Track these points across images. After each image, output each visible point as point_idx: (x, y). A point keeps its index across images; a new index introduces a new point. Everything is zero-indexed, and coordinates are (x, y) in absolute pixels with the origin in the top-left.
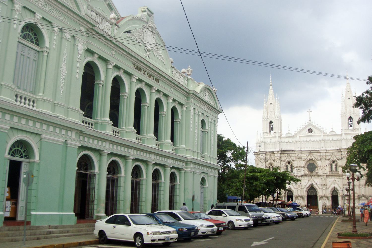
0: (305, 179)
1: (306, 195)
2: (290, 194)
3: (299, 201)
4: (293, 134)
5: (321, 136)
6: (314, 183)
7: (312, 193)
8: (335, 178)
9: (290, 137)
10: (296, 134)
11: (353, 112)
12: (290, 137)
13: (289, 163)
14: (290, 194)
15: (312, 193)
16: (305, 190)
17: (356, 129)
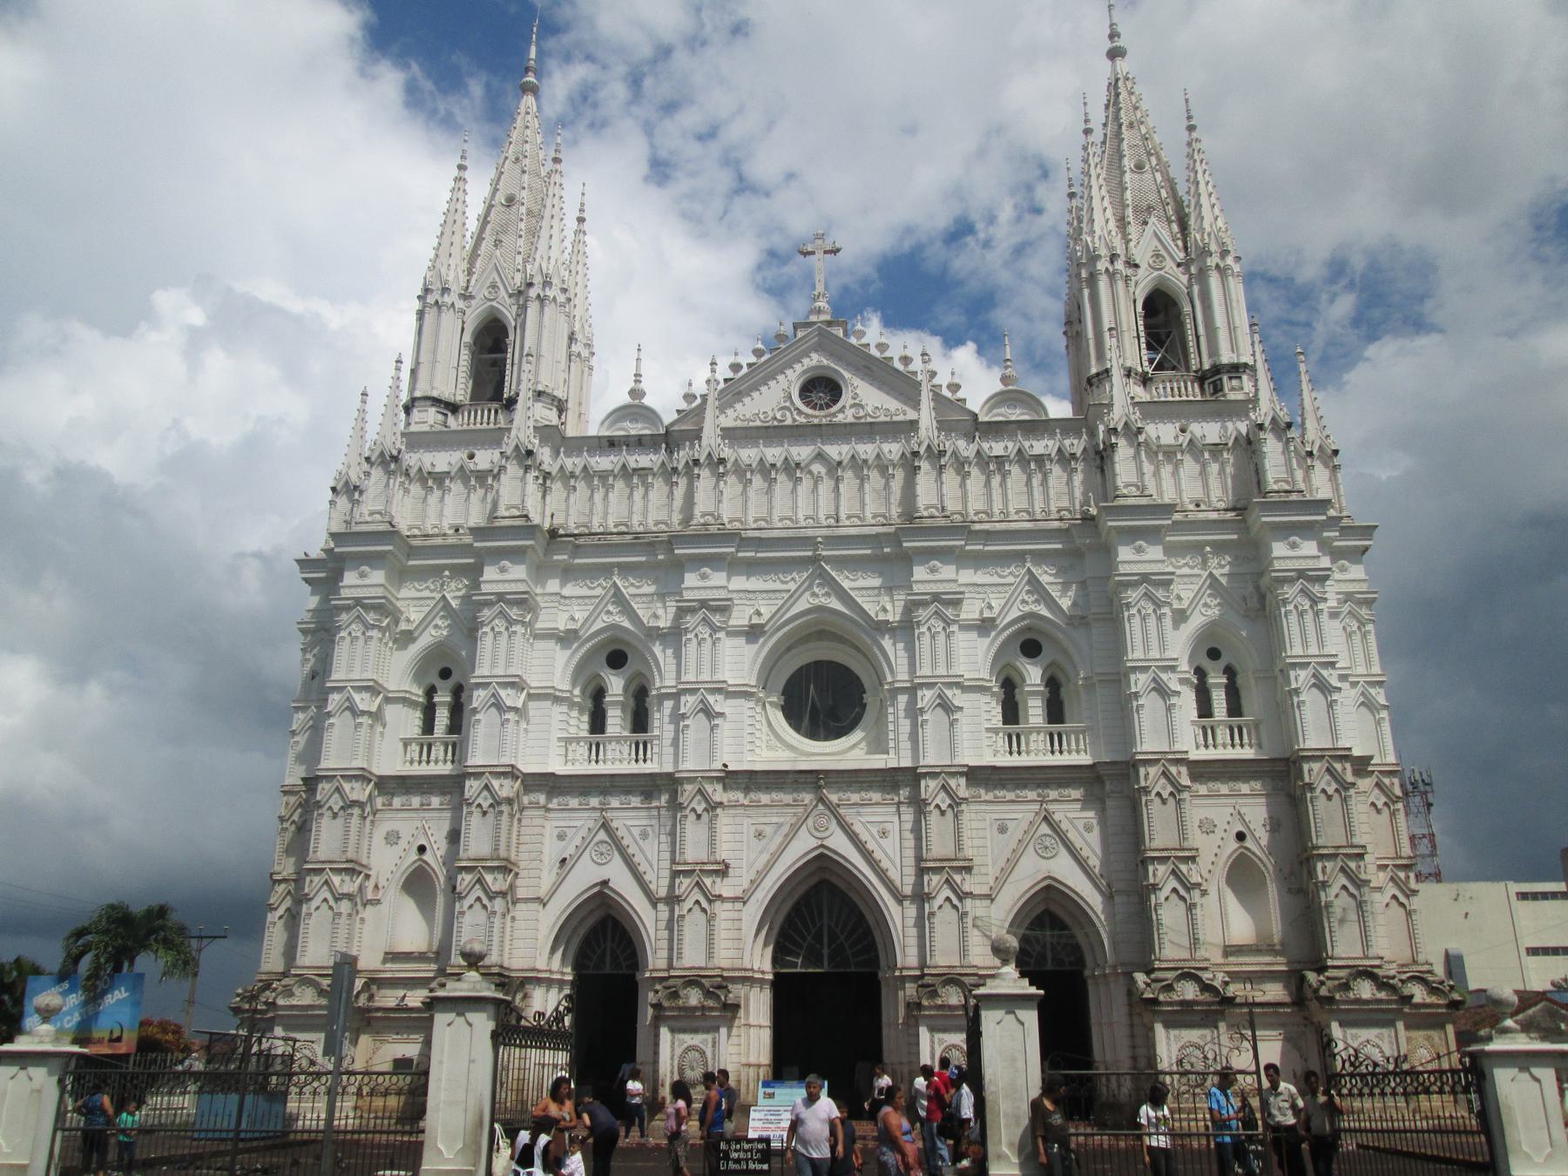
0: (758, 805)
1: (767, 965)
2: (608, 959)
3: (695, 1031)
4: (668, 417)
5: (913, 425)
6: (839, 843)
7: (826, 951)
8: (1053, 794)
9: (639, 443)
10: (693, 414)
11: (1182, 255)
12: (639, 443)
13: (617, 659)
14: (608, 959)
15: (826, 951)
16: (753, 912)
17: (1217, 369)
